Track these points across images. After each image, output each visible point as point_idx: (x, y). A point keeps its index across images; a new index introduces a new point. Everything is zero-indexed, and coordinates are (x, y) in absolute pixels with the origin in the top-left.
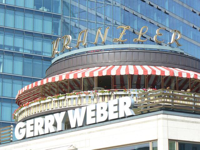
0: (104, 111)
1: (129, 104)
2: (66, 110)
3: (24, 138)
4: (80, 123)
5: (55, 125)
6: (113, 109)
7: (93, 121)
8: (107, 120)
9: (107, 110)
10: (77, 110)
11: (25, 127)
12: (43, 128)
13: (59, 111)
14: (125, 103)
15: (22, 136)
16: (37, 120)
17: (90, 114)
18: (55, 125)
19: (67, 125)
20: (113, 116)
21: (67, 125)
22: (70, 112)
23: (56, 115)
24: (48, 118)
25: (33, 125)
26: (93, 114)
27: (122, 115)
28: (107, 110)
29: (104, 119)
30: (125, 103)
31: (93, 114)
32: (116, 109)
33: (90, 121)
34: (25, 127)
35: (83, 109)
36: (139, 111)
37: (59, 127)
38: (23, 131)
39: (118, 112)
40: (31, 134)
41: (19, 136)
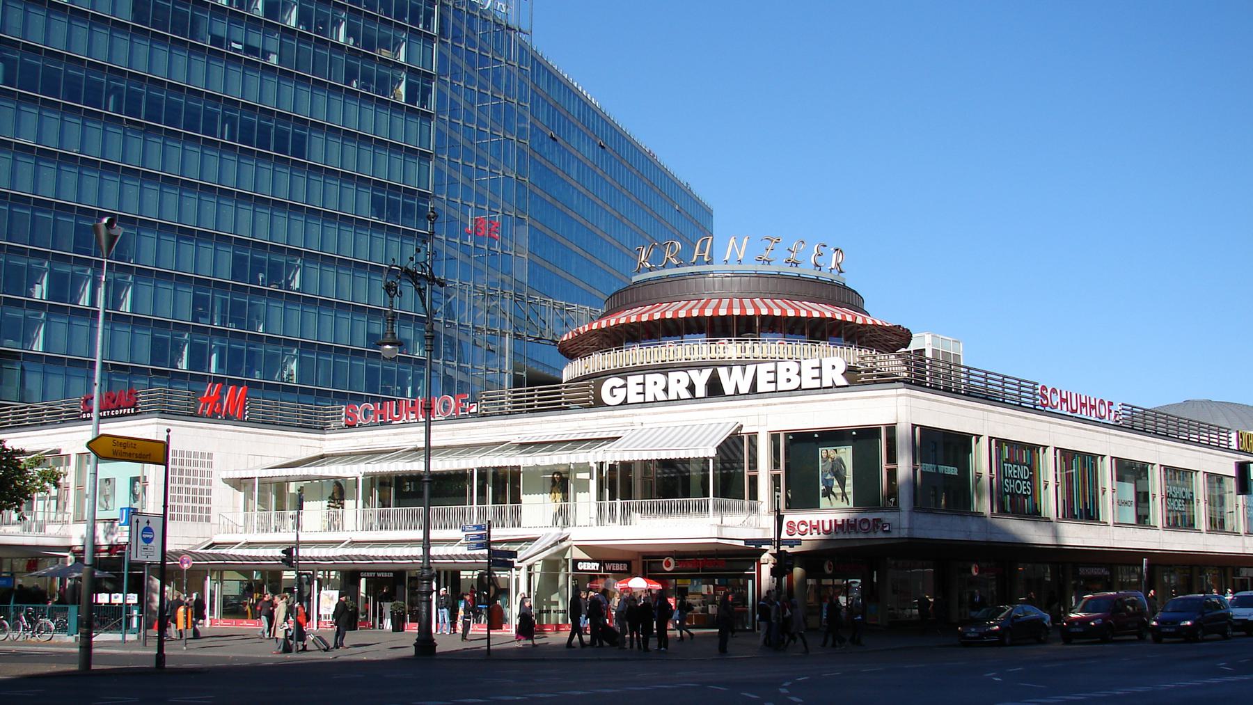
0: (793, 375)
1: (841, 367)
2: (715, 365)
3: (625, 402)
4: (745, 388)
5: (691, 388)
6: (808, 373)
7: (772, 387)
8: (799, 388)
9: (799, 374)
12: (666, 390)
13: (700, 367)
14: (834, 367)
15: (620, 399)
16: (650, 378)
18: (691, 388)
19: (714, 388)
21: (714, 388)
22: (722, 372)
23: (694, 374)
24: (673, 376)
26: (771, 377)
28: (799, 374)
29: (794, 385)
30: (834, 367)
34: (625, 386)
35: (750, 369)
36: (854, 377)
37: (701, 391)
39: (820, 378)
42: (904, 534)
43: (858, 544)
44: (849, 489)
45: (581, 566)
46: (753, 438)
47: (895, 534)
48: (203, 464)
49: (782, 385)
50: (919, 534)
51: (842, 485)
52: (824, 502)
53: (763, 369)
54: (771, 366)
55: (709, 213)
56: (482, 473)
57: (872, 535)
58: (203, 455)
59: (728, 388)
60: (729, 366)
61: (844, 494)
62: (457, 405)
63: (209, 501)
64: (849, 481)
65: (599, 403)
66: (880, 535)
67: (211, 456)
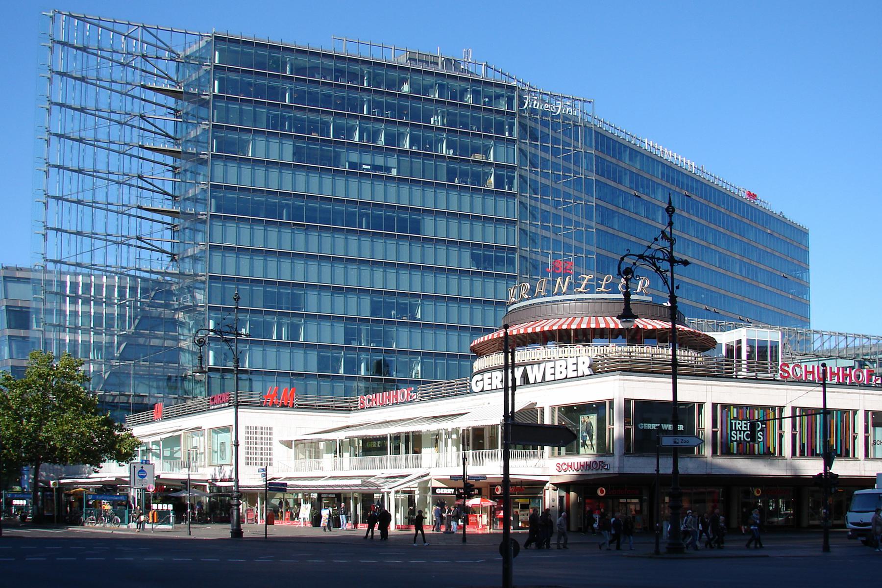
0: (563, 369)
1: (587, 364)
3: (482, 391)
6: (572, 367)
7: (552, 378)
8: (566, 378)
10: (536, 366)
11: (482, 380)
15: (480, 389)
17: (549, 371)
20: (572, 374)
22: (529, 368)
25: (490, 378)
26: (552, 371)
27: (580, 374)
31: (552, 371)
32: (574, 367)
33: (548, 377)
34: (482, 380)
35: (542, 366)
36: (596, 369)
38: (480, 384)
40: (489, 388)
41: (475, 389)
42: (616, 471)
43: (593, 477)
44: (595, 442)
45: (438, 491)
46: (542, 410)
47: (611, 471)
48: (266, 433)
49: (558, 376)
50: (628, 470)
51: (591, 439)
52: (582, 450)
53: (549, 365)
54: (552, 364)
55: (804, 233)
56: (407, 436)
57: (599, 472)
58: (266, 428)
59: (532, 381)
60: (532, 364)
61: (592, 445)
62: (408, 394)
63: (271, 454)
64: (595, 437)
65: (472, 392)
66: (604, 472)
67: (271, 429)
